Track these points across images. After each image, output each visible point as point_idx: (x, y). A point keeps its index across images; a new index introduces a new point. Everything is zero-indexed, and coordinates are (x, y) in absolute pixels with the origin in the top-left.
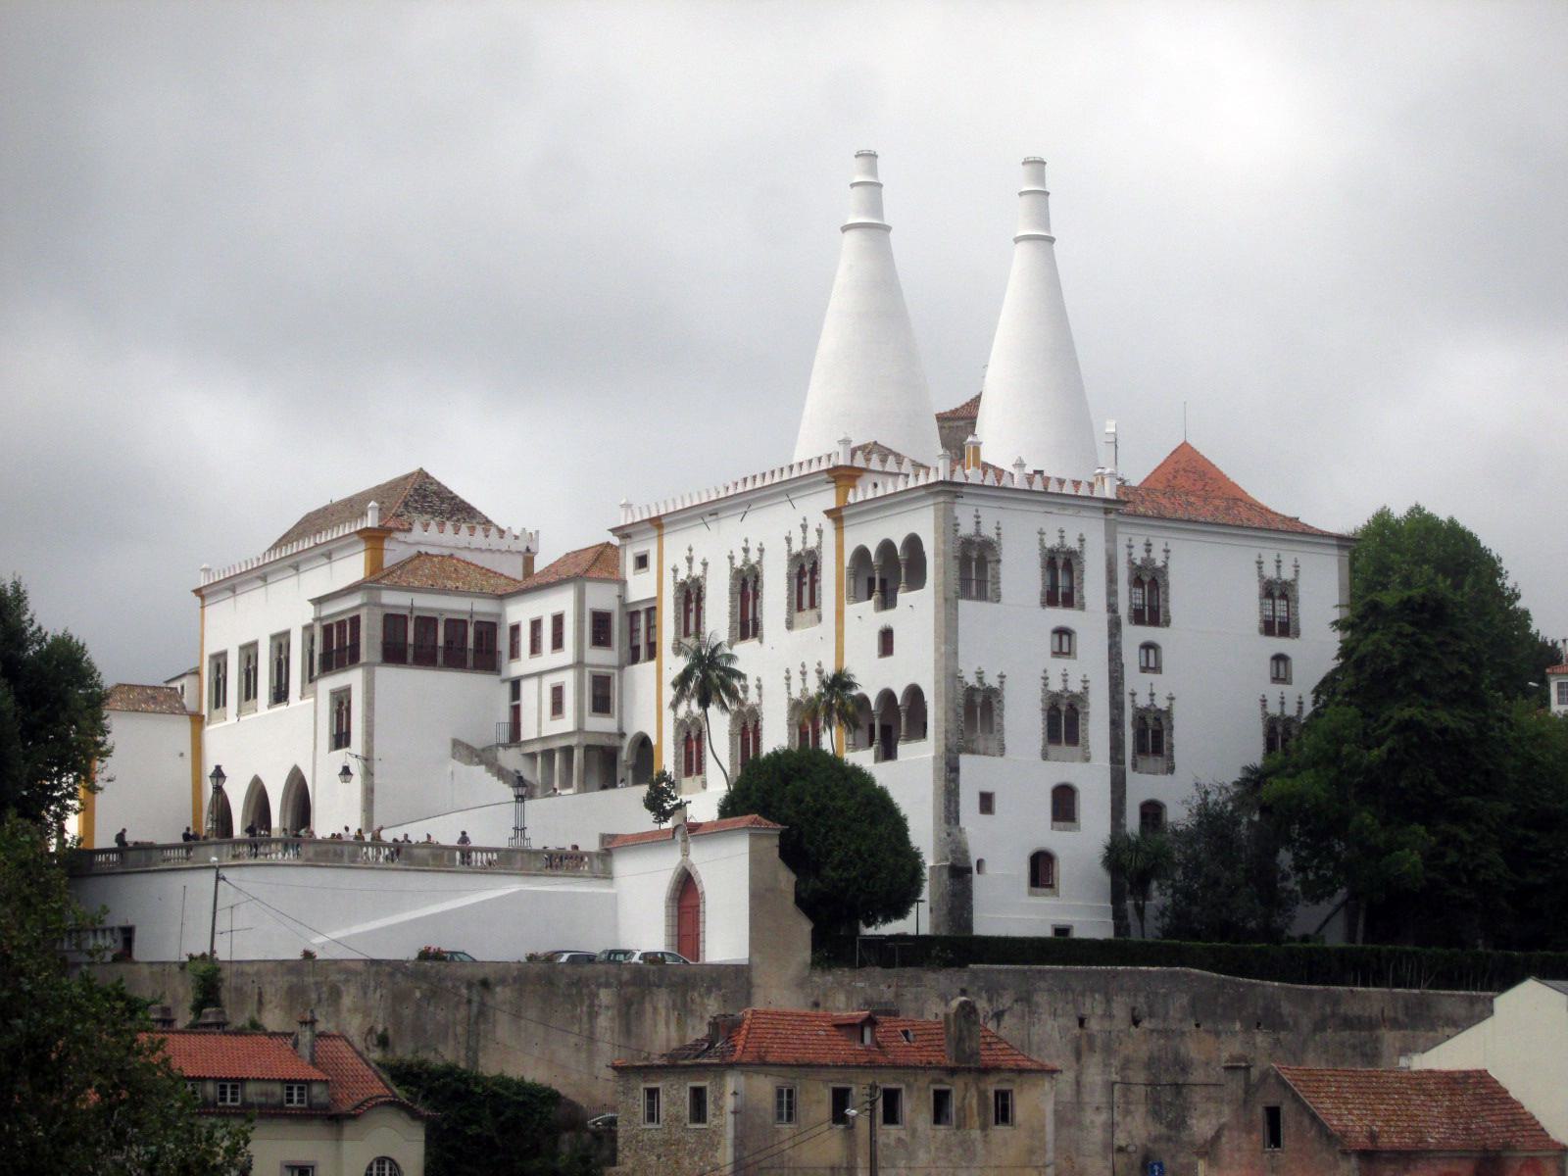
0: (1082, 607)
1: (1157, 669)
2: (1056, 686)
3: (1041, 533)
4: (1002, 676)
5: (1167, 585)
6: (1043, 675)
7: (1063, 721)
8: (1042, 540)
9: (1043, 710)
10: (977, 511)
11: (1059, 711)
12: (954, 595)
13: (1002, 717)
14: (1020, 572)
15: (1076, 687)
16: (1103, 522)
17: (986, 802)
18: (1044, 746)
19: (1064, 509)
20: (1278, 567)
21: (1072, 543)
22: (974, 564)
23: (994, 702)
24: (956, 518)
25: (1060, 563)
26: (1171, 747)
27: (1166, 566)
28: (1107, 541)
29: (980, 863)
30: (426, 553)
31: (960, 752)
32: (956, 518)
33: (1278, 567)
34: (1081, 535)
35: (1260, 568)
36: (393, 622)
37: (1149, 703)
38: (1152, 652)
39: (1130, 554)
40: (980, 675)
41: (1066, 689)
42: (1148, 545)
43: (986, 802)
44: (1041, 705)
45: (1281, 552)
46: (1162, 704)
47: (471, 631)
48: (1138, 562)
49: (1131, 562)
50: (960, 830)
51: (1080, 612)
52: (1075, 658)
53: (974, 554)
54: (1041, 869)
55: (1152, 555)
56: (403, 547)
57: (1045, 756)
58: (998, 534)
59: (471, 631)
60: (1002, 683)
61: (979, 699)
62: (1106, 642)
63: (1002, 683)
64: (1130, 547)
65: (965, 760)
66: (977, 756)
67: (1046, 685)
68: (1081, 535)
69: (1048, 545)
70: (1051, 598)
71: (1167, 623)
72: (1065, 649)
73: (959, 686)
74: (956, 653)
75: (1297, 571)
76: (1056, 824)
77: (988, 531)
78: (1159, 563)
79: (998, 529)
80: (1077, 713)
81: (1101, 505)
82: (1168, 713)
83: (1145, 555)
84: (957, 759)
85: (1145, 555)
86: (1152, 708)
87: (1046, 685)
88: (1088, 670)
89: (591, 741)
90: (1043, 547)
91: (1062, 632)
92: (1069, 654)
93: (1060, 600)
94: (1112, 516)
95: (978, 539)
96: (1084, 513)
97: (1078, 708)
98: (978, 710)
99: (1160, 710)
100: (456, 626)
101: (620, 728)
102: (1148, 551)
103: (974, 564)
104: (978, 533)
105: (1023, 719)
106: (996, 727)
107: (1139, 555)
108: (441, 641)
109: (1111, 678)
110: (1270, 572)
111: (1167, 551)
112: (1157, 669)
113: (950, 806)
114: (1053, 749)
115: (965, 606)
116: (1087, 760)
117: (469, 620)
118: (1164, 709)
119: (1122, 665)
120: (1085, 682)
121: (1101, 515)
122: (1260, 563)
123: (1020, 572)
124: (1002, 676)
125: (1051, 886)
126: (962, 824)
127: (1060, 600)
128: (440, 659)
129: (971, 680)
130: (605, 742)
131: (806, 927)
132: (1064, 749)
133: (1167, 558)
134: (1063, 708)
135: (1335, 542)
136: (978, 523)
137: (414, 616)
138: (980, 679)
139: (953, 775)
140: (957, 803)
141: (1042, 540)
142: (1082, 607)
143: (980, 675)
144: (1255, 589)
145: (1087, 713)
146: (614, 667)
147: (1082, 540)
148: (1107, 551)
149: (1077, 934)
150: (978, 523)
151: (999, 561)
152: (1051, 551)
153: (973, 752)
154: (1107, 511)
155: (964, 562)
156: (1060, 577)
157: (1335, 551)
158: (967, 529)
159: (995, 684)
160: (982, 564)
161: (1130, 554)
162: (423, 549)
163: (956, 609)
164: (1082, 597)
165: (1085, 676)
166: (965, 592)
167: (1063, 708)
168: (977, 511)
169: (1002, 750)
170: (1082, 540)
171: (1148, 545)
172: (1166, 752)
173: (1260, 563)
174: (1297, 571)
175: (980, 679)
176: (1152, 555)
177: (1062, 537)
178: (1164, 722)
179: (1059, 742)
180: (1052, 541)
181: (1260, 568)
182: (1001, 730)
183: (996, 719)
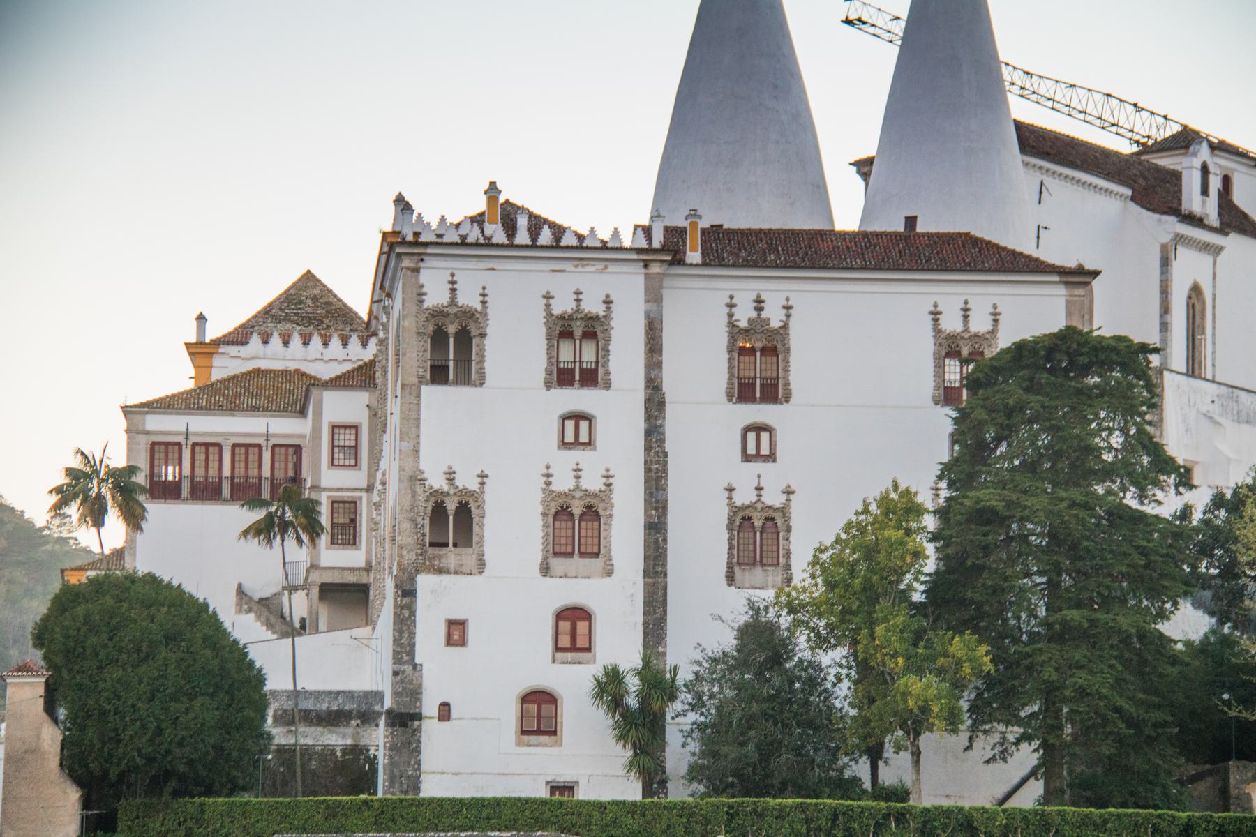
0: (607, 385)
1: (771, 457)
2: (563, 483)
3: (548, 297)
4: (483, 476)
5: (788, 350)
6: (545, 471)
7: (574, 526)
8: (548, 305)
9: (544, 515)
10: (453, 275)
11: (571, 515)
12: (415, 380)
13: (481, 526)
14: (514, 347)
15: (593, 483)
16: (641, 279)
17: (456, 633)
18: (545, 559)
19: (583, 266)
20: (966, 317)
21: (592, 306)
22: (451, 340)
23: (473, 506)
24: (422, 286)
25: (578, 333)
26: (788, 555)
27: (785, 326)
28: (647, 301)
29: (445, 712)
30: (259, 370)
31: (418, 572)
32: (422, 286)
33: (966, 317)
34: (608, 296)
35: (936, 320)
36: (162, 449)
37: (755, 499)
38: (765, 436)
39: (731, 315)
40: (450, 475)
41: (577, 487)
42: (759, 304)
43: (456, 633)
44: (540, 509)
45: (791, 295)
46: (773, 498)
47: (267, 456)
48: (743, 324)
49: (732, 325)
50: (415, 666)
51: (604, 392)
52: (595, 449)
53: (452, 329)
54: (539, 714)
55: (764, 315)
56: (239, 361)
57: (545, 570)
58: (484, 303)
59: (267, 456)
60: (482, 484)
61: (451, 506)
62: (641, 425)
63: (482, 484)
64: (731, 306)
65: (425, 582)
66: (445, 578)
67: (548, 484)
68: (608, 296)
69: (557, 311)
70: (562, 377)
71: (787, 398)
72: (584, 438)
73: (419, 490)
74: (417, 451)
75: (996, 321)
76: (559, 655)
77: (468, 298)
78: (775, 324)
79: (484, 295)
80: (597, 517)
81: (635, 256)
82: (784, 510)
83: (754, 314)
84: (412, 580)
85: (754, 314)
86: (759, 506)
87: (548, 484)
88: (617, 458)
89: (329, 578)
90: (549, 314)
91: (578, 417)
92: (589, 444)
93: (577, 378)
94: (655, 269)
95: (455, 310)
96: (612, 268)
97: (601, 512)
98: (451, 523)
99: (770, 507)
100: (246, 449)
101: (369, 564)
102: (759, 310)
103: (451, 340)
104: (453, 302)
105: (512, 528)
106: (475, 539)
107: (744, 315)
108: (227, 472)
109: (648, 470)
110: (951, 323)
111: (788, 308)
112: (771, 457)
113: (401, 637)
114: (557, 564)
115: (431, 394)
116: (609, 573)
117: (264, 443)
118: (777, 505)
119: (666, 455)
120: (608, 477)
121: (639, 268)
122: (935, 315)
123: (514, 347)
124: (483, 476)
125: (554, 733)
126: (417, 661)
127: (577, 378)
128: (186, 491)
129: (437, 481)
130: (351, 578)
131: (73, 795)
132: (577, 563)
133: (788, 316)
134: (577, 512)
135: (1056, 278)
136: (453, 290)
137: (190, 443)
138: (451, 480)
139: (406, 600)
140: (412, 635)
141: (548, 305)
142: (607, 385)
143: (450, 475)
144: (927, 346)
145: (611, 516)
146: (361, 490)
147: (608, 302)
148: (647, 315)
149: (582, 794)
150: (453, 290)
151: (483, 335)
152: (561, 317)
153: (440, 571)
154: (646, 264)
155: (438, 338)
156: (576, 350)
157: (1062, 291)
158: (436, 296)
159: (473, 485)
160: (464, 339)
161: (731, 315)
162: (264, 365)
163: (419, 396)
164: (608, 373)
165: (608, 470)
166: (438, 375)
167: (577, 512)
168: (453, 275)
169: (481, 564)
170: (608, 302)
171: (759, 304)
172: (782, 560)
173: (935, 315)
174: (996, 321)
175: (451, 480)
176: (764, 315)
177: (578, 300)
178: (779, 521)
179: (571, 555)
180: (564, 305)
181: (936, 320)
182: (481, 543)
183: (476, 529)
